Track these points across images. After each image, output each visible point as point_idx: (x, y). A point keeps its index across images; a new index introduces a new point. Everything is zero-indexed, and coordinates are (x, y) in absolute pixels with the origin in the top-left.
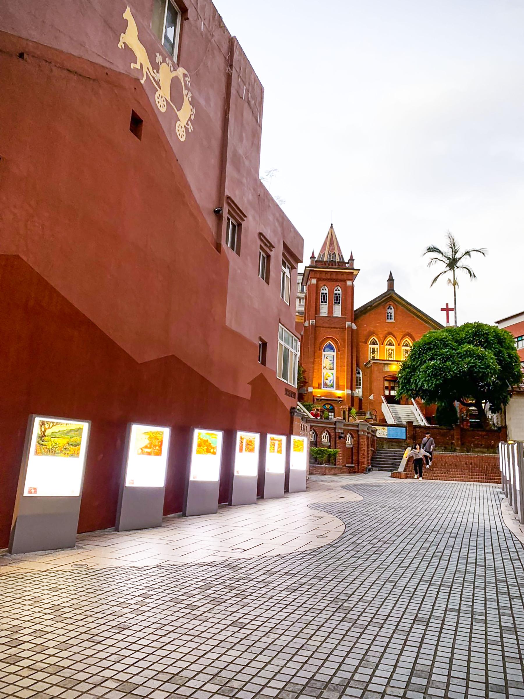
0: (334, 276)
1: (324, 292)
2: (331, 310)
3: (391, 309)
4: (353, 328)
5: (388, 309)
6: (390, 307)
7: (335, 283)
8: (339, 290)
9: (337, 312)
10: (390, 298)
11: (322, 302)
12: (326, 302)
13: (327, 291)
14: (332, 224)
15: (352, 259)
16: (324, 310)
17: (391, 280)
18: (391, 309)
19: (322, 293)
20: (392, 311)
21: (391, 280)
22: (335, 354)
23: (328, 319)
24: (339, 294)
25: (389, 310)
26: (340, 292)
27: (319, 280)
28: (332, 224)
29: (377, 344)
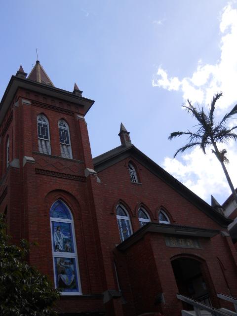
0: (58, 105)
2: (55, 147)
3: (131, 169)
6: (129, 166)
9: (67, 153)
12: (47, 138)
13: (47, 123)
14: (38, 62)
17: (124, 134)
18: (131, 169)
20: (133, 171)
21: (124, 134)
22: (70, 221)
28: (38, 62)
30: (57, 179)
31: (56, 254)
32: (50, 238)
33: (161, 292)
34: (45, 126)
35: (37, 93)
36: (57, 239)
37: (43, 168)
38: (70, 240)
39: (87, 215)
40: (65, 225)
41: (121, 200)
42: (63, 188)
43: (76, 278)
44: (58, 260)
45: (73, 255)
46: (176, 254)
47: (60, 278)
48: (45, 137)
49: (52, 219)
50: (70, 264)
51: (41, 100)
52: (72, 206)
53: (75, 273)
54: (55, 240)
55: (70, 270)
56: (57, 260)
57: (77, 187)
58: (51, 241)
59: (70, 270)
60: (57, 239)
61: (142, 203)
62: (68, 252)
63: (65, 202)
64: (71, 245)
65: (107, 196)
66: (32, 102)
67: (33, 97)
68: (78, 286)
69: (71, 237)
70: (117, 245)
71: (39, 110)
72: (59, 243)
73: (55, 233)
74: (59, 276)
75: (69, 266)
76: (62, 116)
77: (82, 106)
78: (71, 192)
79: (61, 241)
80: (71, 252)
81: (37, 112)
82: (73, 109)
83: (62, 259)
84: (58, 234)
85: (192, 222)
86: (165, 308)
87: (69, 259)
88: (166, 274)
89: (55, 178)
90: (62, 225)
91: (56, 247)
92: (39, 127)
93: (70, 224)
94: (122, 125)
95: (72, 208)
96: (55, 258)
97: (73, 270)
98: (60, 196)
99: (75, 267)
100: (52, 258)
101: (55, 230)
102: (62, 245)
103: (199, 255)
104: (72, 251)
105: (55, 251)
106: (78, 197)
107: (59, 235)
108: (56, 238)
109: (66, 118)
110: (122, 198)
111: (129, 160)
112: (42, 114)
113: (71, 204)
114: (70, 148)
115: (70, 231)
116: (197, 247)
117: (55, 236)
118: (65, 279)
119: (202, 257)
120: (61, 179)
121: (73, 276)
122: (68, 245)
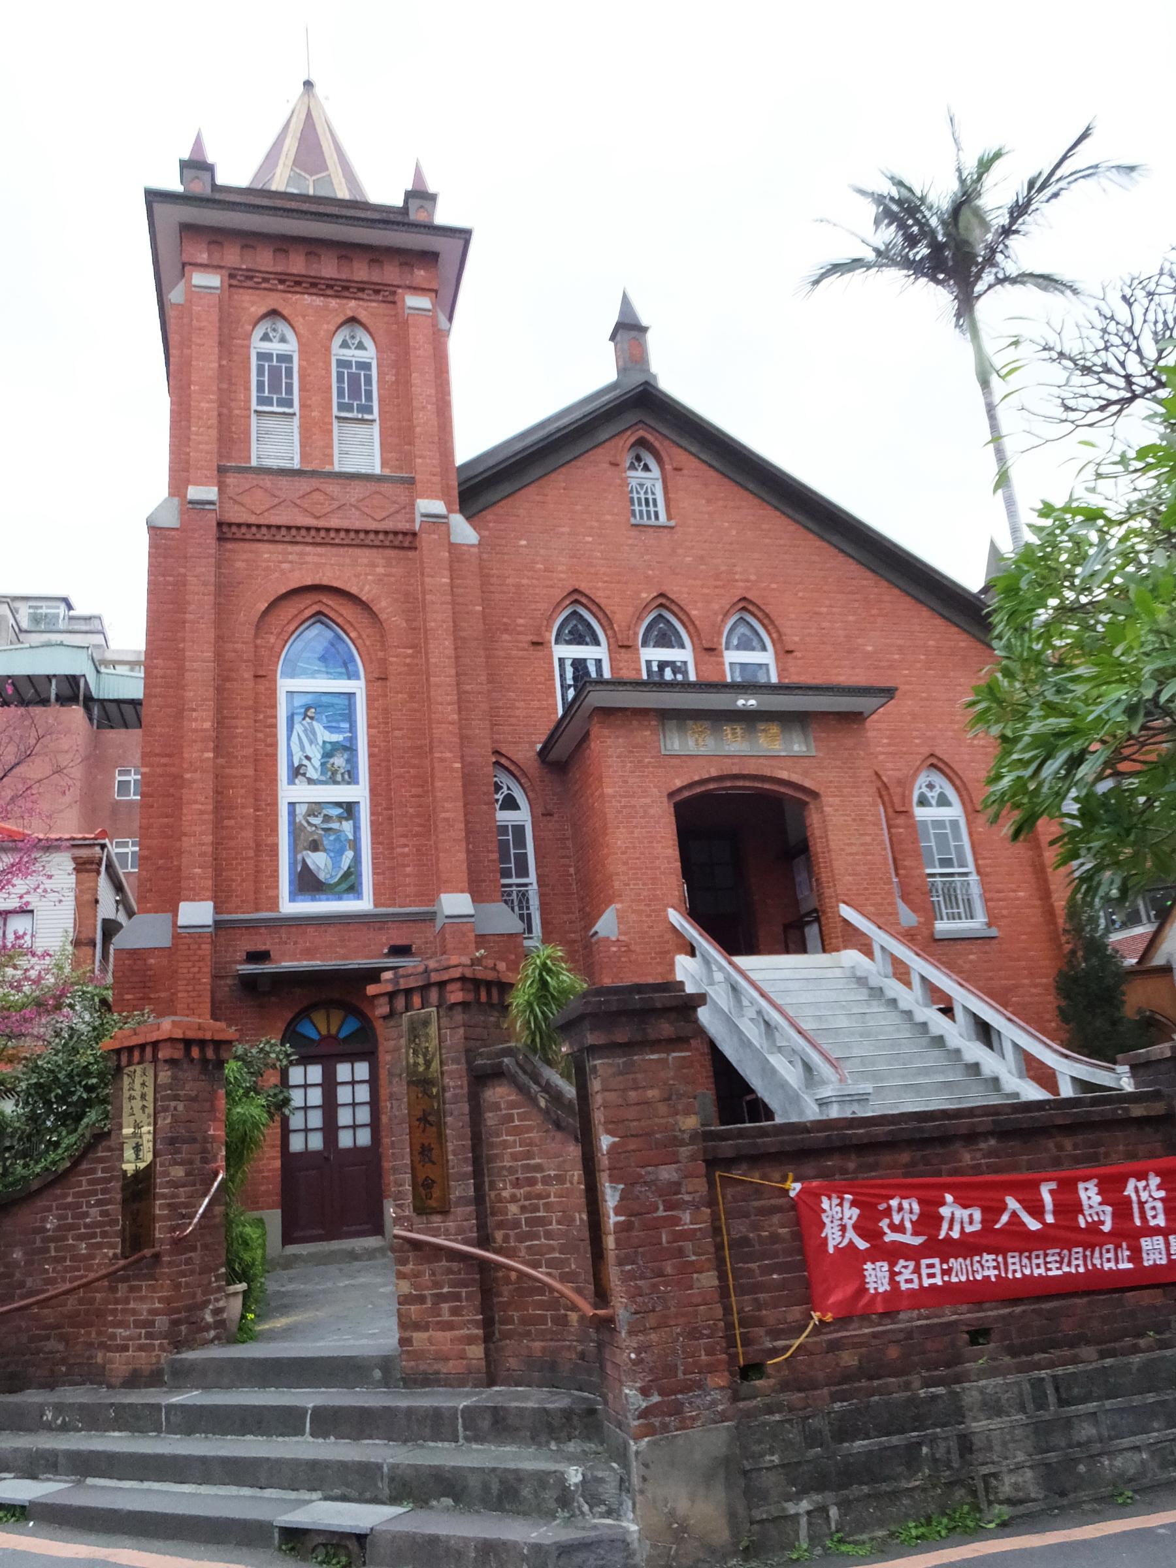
1: (275, 347)
3: (646, 468)
4: (455, 539)
5: (632, 467)
6: (638, 458)
7: (333, 303)
8: (360, 346)
9: (360, 450)
10: (639, 415)
11: (262, 401)
12: (290, 404)
13: (291, 347)
14: (308, 84)
15: (420, 195)
16: (276, 444)
18: (646, 468)
19: (263, 356)
22: (357, 687)
23: (304, 485)
24: (366, 366)
25: (636, 476)
26: (369, 354)
27: (238, 279)
28: (308, 84)
29: (598, 643)
30: (309, 549)
31: (292, 794)
32: (274, 745)
33: (611, 902)
34: (286, 358)
35: (250, 239)
36: (303, 748)
37: (262, 521)
38: (349, 748)
39: (408, 661)
40: (335, 700)
41: (576, 591)
42: (327, 578)
43: (357, 860)
44: (301, 810)
45: (359, 793)
46: (697, 778)
47: (304, 860)
48: (281, 403)
49: (285, 685)
50: (340, 818)
51: (264, 260)
52: (360, 636)
53: (355, 845)
54: (295, 748)
55: (338, 839)
56: (298, 811)
57: (380, 570)
58: (274, 757)
59: (338, 839)
60: (303, 748)
61: (662, 595)
62: (336, 782)
63: (338, 625)
64: (348, 761)
65: (525, 581)
66: (231, 276)
67: (232, 256)
68: (361, 884)
69: (353, 739)
70: (539, 747)
71: (253, 303)
72: (308, 758)
73: (298, 728)
74: (299, 857)
75: (335, 825)
76: (352, 307)
77: (430, 258)
78: (354, 590)
79: (316, 754)
80: (349, 783)
81: (253, 309)
82: (390, 274)
83: (315, 808)
84: (305, 730)
85: (870, 648)
86: (614, 949)
87: (339, 804)
88: (915, 798)
89: (298, 548)
90: (324, 699)
91: (296, 772)
92: (260, 372)
93: (351, 696)
94: (626, 302)
95: (359, 642)
96: (292, 805)
97: (351, 837)
98: (316, 608)
99: (356, 829)
100: (274, 804)
101: (297, 719)
102: (317, 762)
103: (795, 778)
104: (351, 777)
105: (291, 782)
106: (384, 606)
107: (311, 734)
108: (297, 742)
109: (363, 315)
110: (583, 587)
111: (632, 440)
112: (274, 313)
113: (355, 629)
114: (376, 427)
115: (350, 717)
116: (798, 748)
117: (294, 738)
118: (322, 866)
119: (807, 783)
120: (319, 550)
121: (350, 854)
122: (339, 761)
